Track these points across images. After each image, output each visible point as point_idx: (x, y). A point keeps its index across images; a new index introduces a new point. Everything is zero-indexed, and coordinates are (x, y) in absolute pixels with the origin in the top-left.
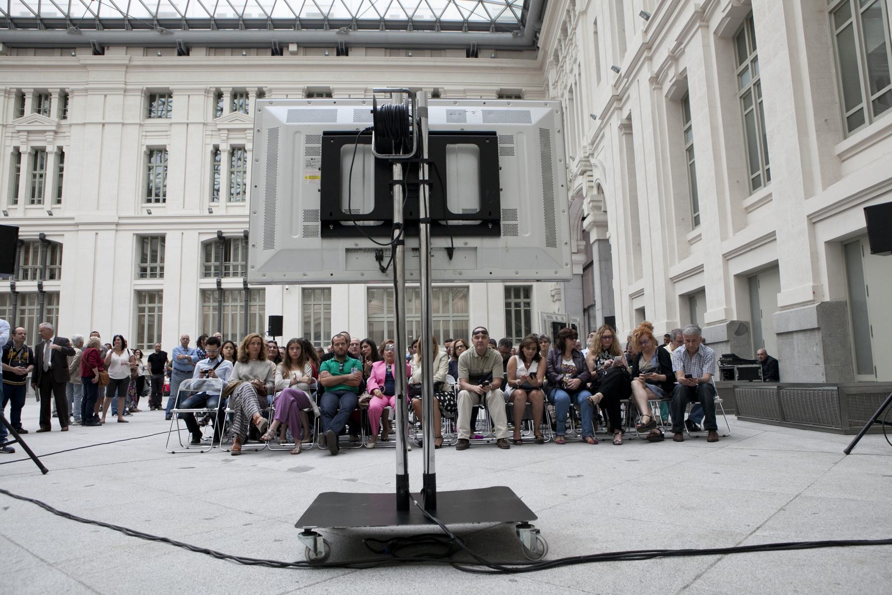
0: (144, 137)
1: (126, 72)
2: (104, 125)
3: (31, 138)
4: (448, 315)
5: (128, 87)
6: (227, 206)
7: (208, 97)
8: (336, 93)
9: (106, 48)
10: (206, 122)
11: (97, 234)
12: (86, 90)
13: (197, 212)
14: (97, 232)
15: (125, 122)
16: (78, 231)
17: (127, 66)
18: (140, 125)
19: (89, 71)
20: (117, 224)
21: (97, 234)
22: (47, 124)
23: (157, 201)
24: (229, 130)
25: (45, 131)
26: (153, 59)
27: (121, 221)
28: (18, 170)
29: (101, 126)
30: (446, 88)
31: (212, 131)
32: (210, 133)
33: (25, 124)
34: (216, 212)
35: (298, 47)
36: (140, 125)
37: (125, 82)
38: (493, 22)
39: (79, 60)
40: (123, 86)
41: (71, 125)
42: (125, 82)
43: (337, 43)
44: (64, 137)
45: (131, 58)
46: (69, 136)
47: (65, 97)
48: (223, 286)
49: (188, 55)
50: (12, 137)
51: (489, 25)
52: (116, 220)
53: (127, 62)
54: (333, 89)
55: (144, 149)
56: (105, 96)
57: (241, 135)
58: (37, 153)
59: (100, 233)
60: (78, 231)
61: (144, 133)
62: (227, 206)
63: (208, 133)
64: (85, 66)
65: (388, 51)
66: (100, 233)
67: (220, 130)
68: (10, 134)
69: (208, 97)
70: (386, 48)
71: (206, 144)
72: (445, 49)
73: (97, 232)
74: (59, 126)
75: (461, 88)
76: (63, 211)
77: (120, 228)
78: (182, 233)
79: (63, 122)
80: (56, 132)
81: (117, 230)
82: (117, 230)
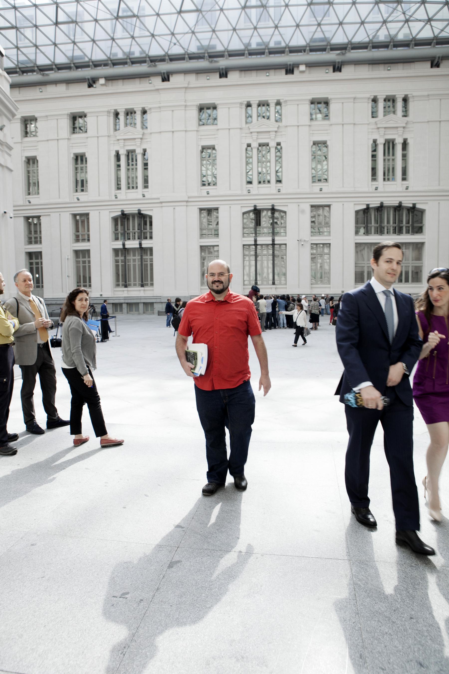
0: (200, 140)
1: (185, 93)
2: (173, 132)
3: (386, 133)
4: (408, 262)
5: (188, 104)
6: (258, 187)
7: (242, 108)
8: (333, 101)
9: (170, 76)
10: (242, 127)
11: (174, 208)
12: (160, 107)
13: (239, 192)
14: (174, 207)
15: (188, 129)
16: (162, 207)
17: (186, 88)
18: (197, 131)
19: (160, 94)
20: (187, 202)
21: (174, 208)
22: (136, 133)
23: (133, 188)
24: (258, 132)
25: (135, 139)
26: (203, 81)
27: (190, 200)
28: (119, 166)
29: (171, 133)
30: (414, 94)
31: (246, 133)
32: (244, 135)
33: (122, 134)
34: (253, 192)
35: (306, 66)
36: (197, 131)
37: (185, 100)
38: (436, 38)
39: (155, 86)
40: (183, 103)
41: (151, 133)
42: (185, 100)
43: (287, 65)
44: (147, 142)
45: (189, 82)
46: (150, 141)
47: (405, 100)
48: (276, 242)
49: (169, 80)
50: (114, 144)
51: (431, 41)
52: (187, 199)
53: (186, 86)
54: (331, 99)
55: (200, 148)
56: (173, 111)
57: (266, 136)
58: (128, 153)
59: (176, 208)
60: (162, 207)
61: (200, 137)
62: (258, 187)
63: (244, 135)
64: (158, 90)
65: (371, 66)
66: (176, 208)
67: (251, 133)
68: (112, 142)
69: (242, 108)
70: (369, 64)
71: (242, 143)
72: (413, 62)
73: (174, 207)
74: (143, 134)
75: (426, 93)
76: (149, 193)
77: (189, 204)
78: (230, 207)
79: (145, 131)
80: (141, 139)
81: (187, 206)
82: (187, 206)
